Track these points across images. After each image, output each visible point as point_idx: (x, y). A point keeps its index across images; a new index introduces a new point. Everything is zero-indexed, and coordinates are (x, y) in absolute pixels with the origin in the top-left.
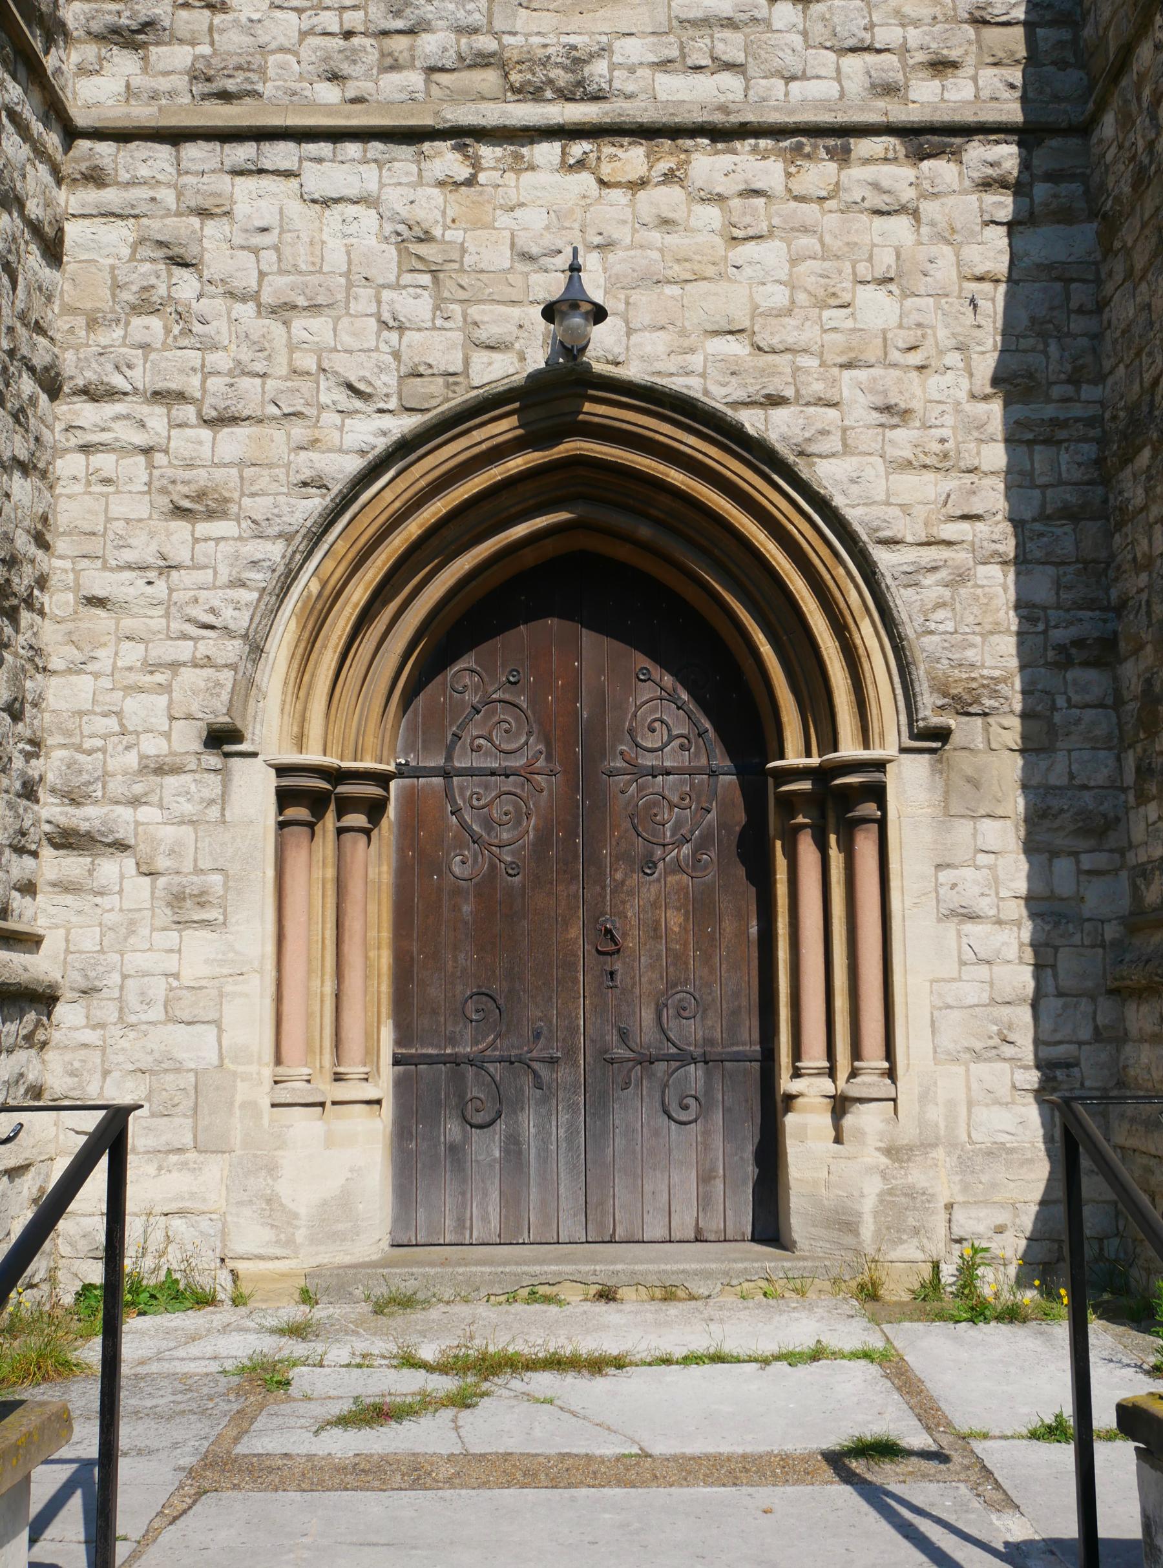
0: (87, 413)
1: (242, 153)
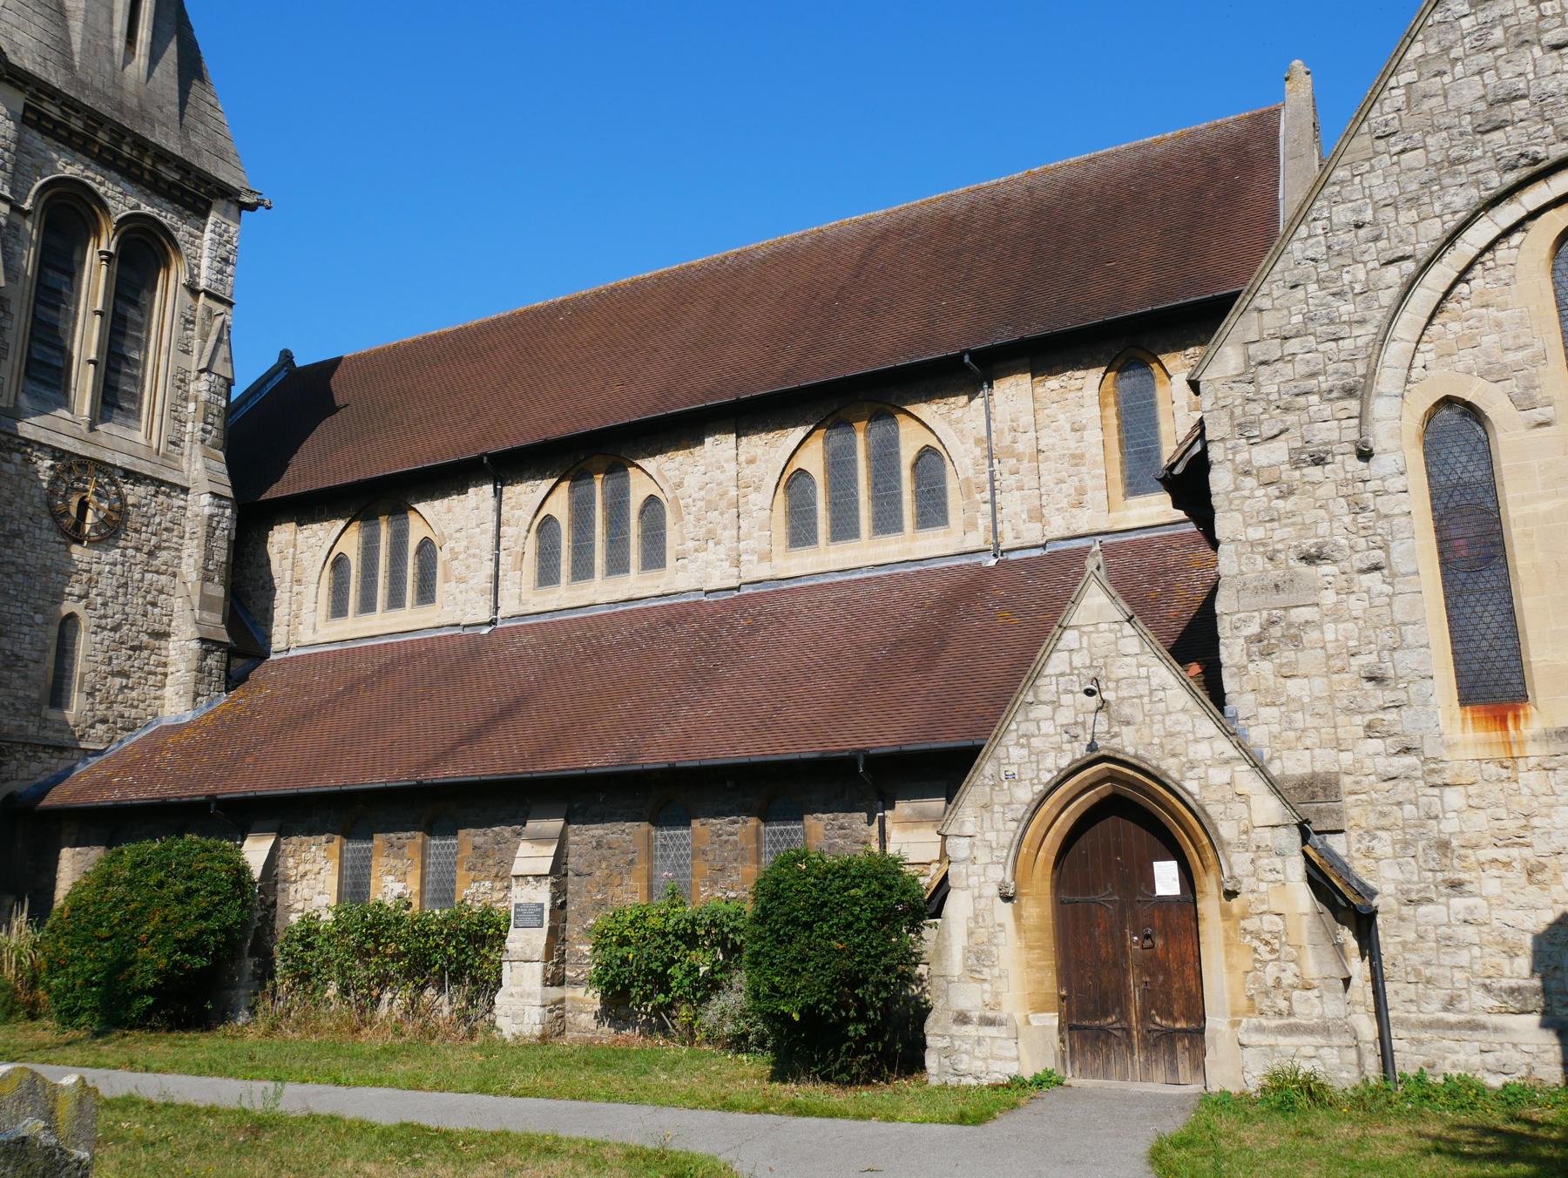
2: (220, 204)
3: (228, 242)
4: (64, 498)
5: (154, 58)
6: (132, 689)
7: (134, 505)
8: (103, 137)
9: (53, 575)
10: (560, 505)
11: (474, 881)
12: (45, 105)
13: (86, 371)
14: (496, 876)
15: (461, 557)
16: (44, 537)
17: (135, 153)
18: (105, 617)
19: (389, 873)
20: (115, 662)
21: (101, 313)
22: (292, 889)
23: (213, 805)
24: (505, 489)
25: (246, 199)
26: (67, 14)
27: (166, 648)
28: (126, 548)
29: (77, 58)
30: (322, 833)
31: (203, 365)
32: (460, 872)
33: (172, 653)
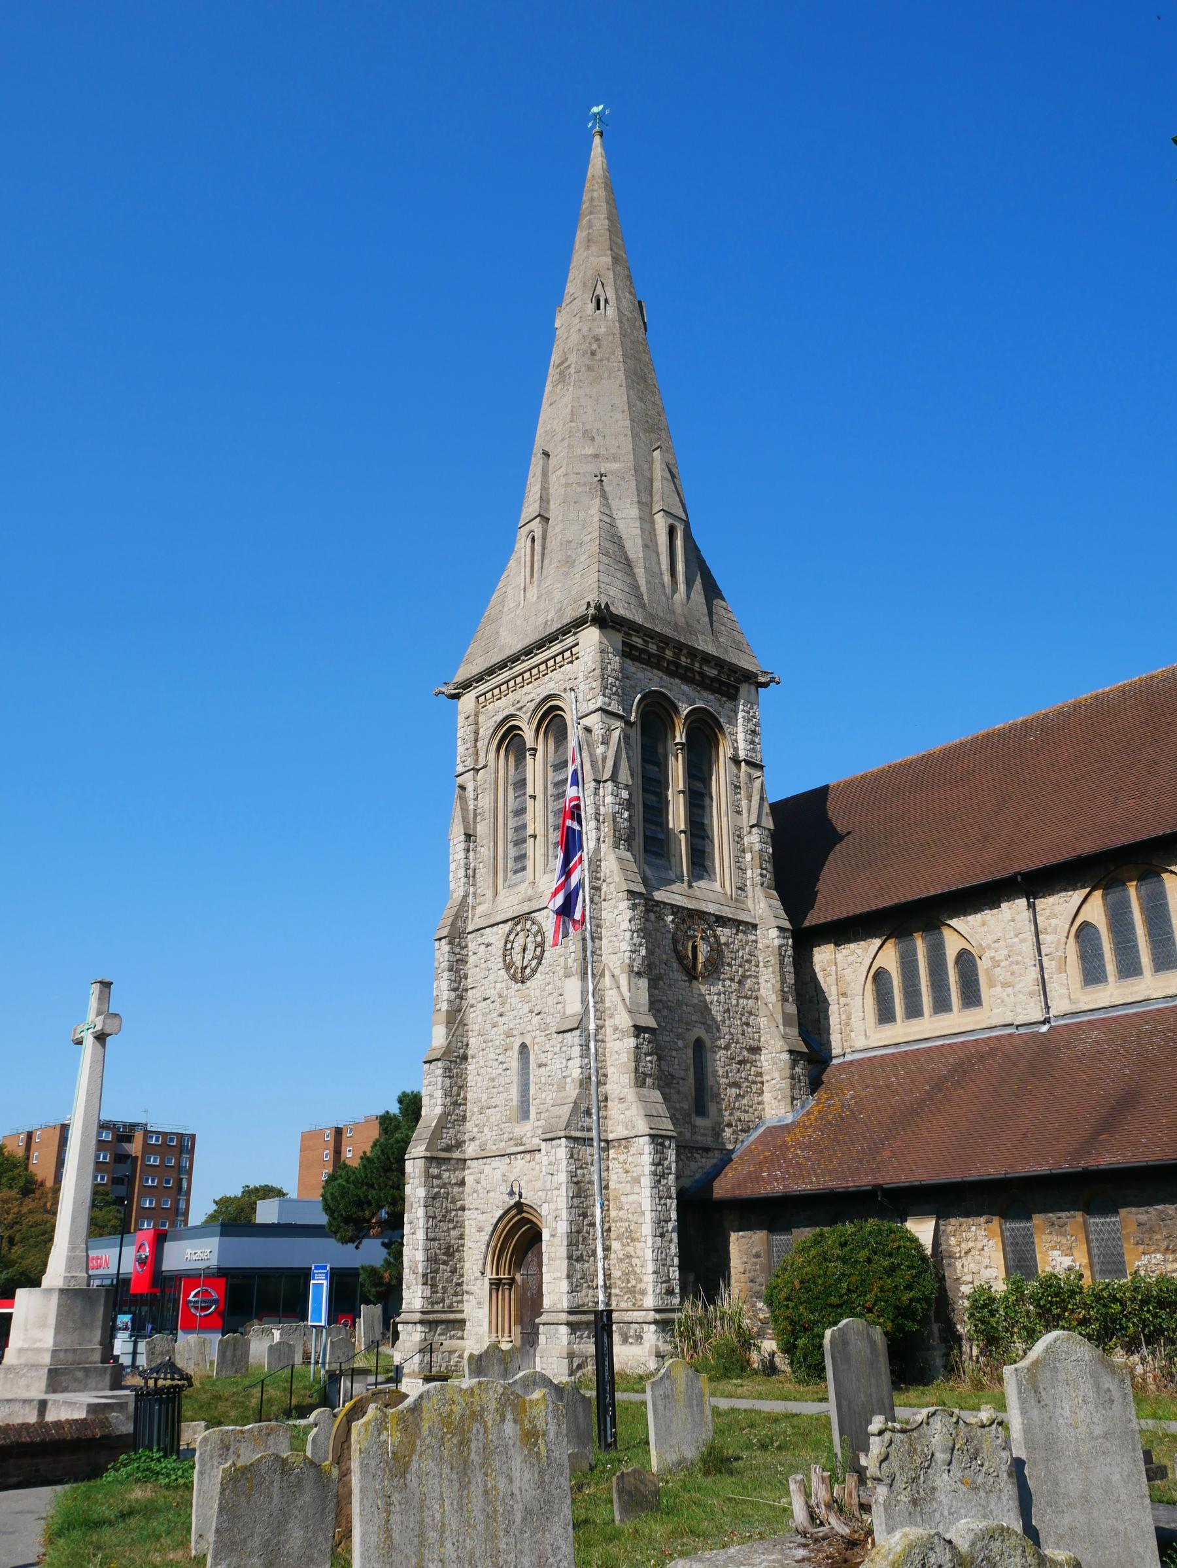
2: (744, 689)
3: (753, 717)
5: (689, 584)
6: (743, 1097)
7: (725, 944)
8: (669, 654)
9: (684, 1007)
10: (1096, 911)
11: (1144, 1254)
12: (634, 639)
14: (1167, 1249)
15: (1002, 964)
16: (675, 977)
17: (689, 661)
19: (1054, 1248)
21: (683, 792)
22: (958, 1264)
23: (879, 1193)
24: (1037, 901)
25: (762, 680)
26: (632, 564)
27: (760, 1060)
28: (724, 980)
29: (645, 597)
30: (981, 1215)
31: (754, 822)
32: (1128, 1247)
33: (765, 1064)
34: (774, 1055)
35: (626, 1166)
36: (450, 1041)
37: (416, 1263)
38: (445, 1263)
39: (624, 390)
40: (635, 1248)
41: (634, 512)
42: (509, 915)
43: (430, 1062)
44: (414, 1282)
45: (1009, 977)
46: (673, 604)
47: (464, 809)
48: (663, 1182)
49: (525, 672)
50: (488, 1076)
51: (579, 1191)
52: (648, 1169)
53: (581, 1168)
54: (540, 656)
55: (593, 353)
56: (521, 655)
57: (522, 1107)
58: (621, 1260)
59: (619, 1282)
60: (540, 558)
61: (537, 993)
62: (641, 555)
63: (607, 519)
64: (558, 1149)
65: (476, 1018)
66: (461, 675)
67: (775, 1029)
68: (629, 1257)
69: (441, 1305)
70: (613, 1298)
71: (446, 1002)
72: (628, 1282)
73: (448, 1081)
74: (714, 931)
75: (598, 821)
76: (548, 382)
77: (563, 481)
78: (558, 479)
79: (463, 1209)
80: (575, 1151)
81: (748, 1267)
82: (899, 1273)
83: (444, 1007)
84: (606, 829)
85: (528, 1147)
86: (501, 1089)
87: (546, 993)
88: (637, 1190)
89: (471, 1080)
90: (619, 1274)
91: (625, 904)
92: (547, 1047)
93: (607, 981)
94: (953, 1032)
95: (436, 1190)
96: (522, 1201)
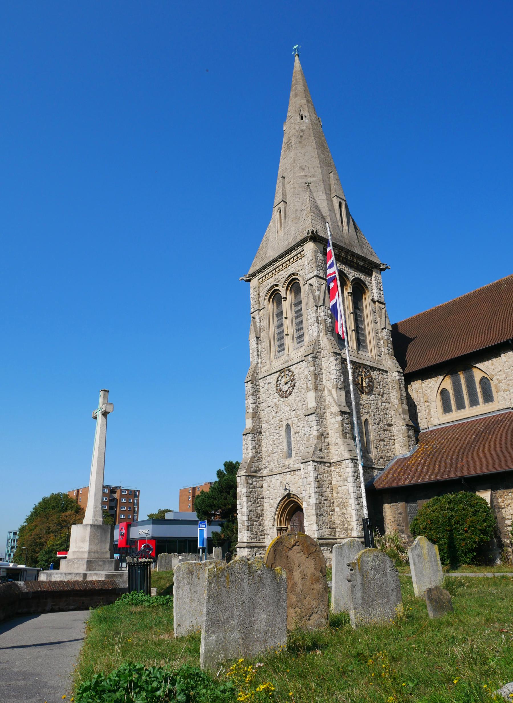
0: (265, 500)
1: (272, 476)
2: (375, 270)
3: (380, 283)
4: (357, 378)
7: (375, 379)
8: (343, 254)
13: (352, 334)
15: (503, 381)
17: (351, 258)
18: (375, 420)
20: (380, 436)
21: (353, 313)
22: (503, 511)
23: (463, 480)
25: (382, 267)
27: (392, 430)
31: (384, 327)
33: (395, 431)
34: (399, 427)
35: (340, 474)
36: (254, 425)
37: (244, 521)
38: (256, 521)
39: (315, 149)
40: (346, 510)
41: (324, 197)
42: (278, 369)
43: (245, 435)
44: (243, 530)
45: (506, 386)
46: (343, 234)
47: (255, 327)
48: (358, 480)
49: (280, 266)
50: (271, 440)
51: (319, 484)
52: (351, 474)
53: (319, 475)
54: (287, 258)
55: (301, 137)
56: (278, 259)
57: (288, 452)
58: (340, 516)
59: (339, 526)
60: (284, 218)
61: (293, 401)
62: (328, 214)
63: (312, 199)
64: (309, 467)
65: (265, 415)
66: (251, 271)
67: (399, 416)
68: (343, 514)
69: (255, 540)
70: (337, 533)
71: (251, 409)
72: (344, 525)
73: (254, 442)
74: (370, 373)
75: (318, 323)
76: (282, 151)
77: (292, 186)
78: (290, 186)
79: (263, 498)
80: (317, 467)
81: (396, 519)
82: (478, 514)
83: (251, 411)
84: (321, 327)
85: (292, 469)
86: (278, 445)
87: (297, 401)
88: (346, 484)
89: (264, 442)
90: (339, 522)
91: (332, 359)
92: (299, 425)
93: (326, 393)
94: (481, 413)
95: (251, 489)
96: (290, 492)
